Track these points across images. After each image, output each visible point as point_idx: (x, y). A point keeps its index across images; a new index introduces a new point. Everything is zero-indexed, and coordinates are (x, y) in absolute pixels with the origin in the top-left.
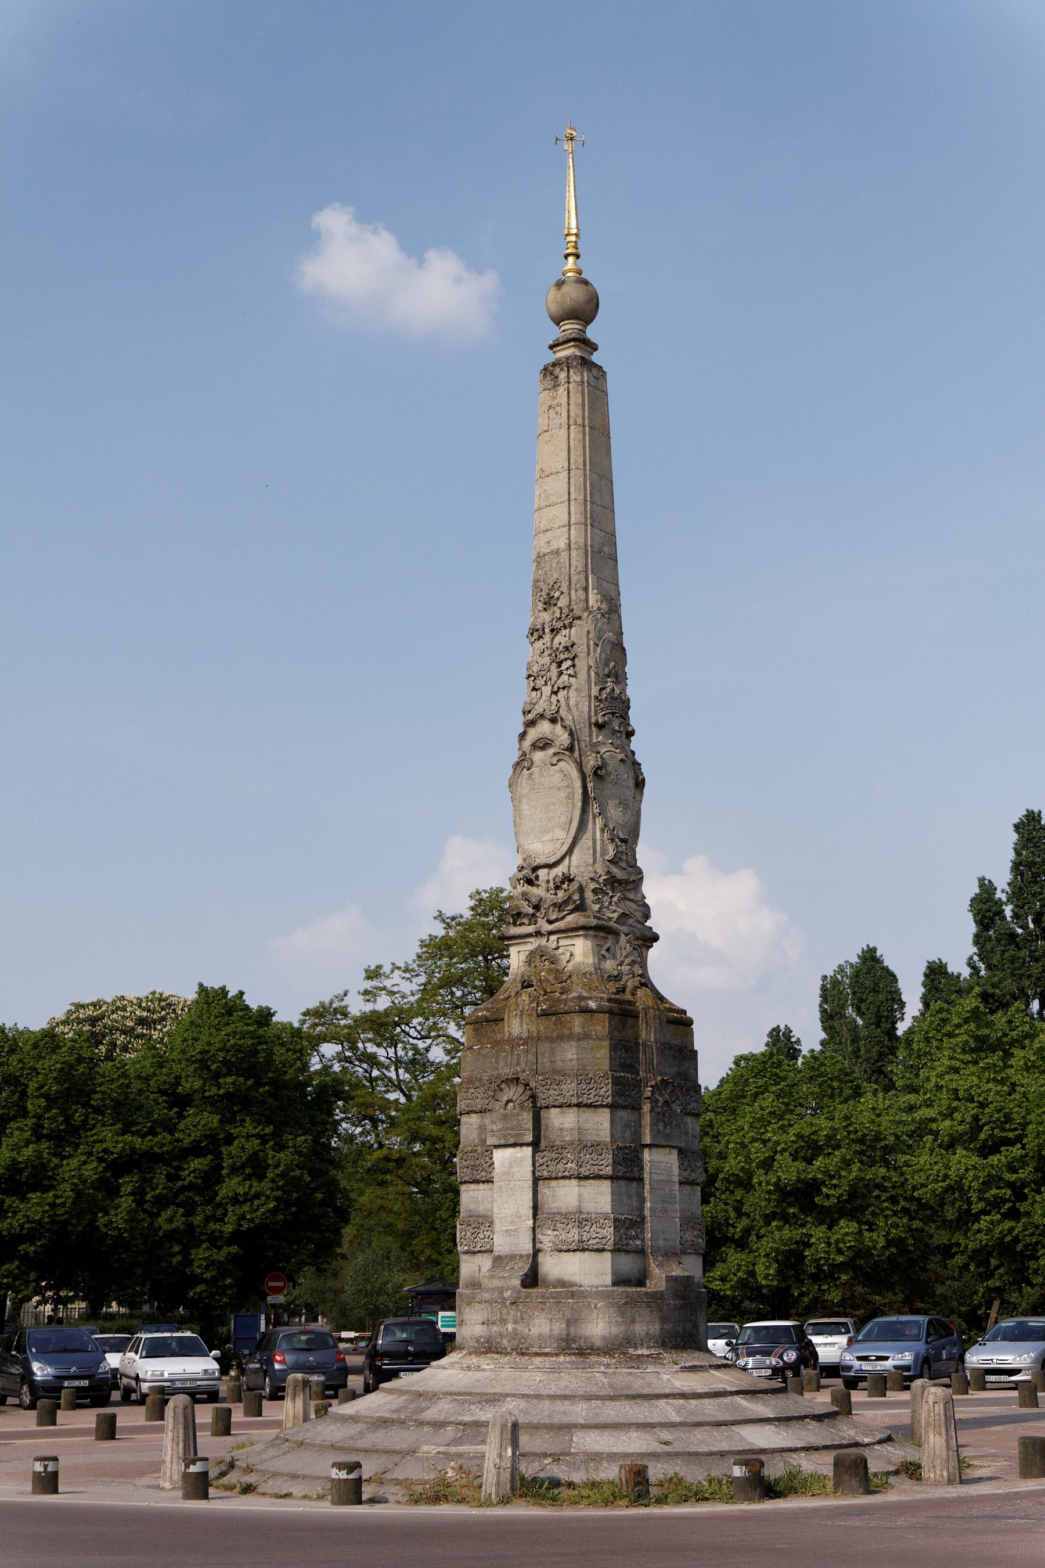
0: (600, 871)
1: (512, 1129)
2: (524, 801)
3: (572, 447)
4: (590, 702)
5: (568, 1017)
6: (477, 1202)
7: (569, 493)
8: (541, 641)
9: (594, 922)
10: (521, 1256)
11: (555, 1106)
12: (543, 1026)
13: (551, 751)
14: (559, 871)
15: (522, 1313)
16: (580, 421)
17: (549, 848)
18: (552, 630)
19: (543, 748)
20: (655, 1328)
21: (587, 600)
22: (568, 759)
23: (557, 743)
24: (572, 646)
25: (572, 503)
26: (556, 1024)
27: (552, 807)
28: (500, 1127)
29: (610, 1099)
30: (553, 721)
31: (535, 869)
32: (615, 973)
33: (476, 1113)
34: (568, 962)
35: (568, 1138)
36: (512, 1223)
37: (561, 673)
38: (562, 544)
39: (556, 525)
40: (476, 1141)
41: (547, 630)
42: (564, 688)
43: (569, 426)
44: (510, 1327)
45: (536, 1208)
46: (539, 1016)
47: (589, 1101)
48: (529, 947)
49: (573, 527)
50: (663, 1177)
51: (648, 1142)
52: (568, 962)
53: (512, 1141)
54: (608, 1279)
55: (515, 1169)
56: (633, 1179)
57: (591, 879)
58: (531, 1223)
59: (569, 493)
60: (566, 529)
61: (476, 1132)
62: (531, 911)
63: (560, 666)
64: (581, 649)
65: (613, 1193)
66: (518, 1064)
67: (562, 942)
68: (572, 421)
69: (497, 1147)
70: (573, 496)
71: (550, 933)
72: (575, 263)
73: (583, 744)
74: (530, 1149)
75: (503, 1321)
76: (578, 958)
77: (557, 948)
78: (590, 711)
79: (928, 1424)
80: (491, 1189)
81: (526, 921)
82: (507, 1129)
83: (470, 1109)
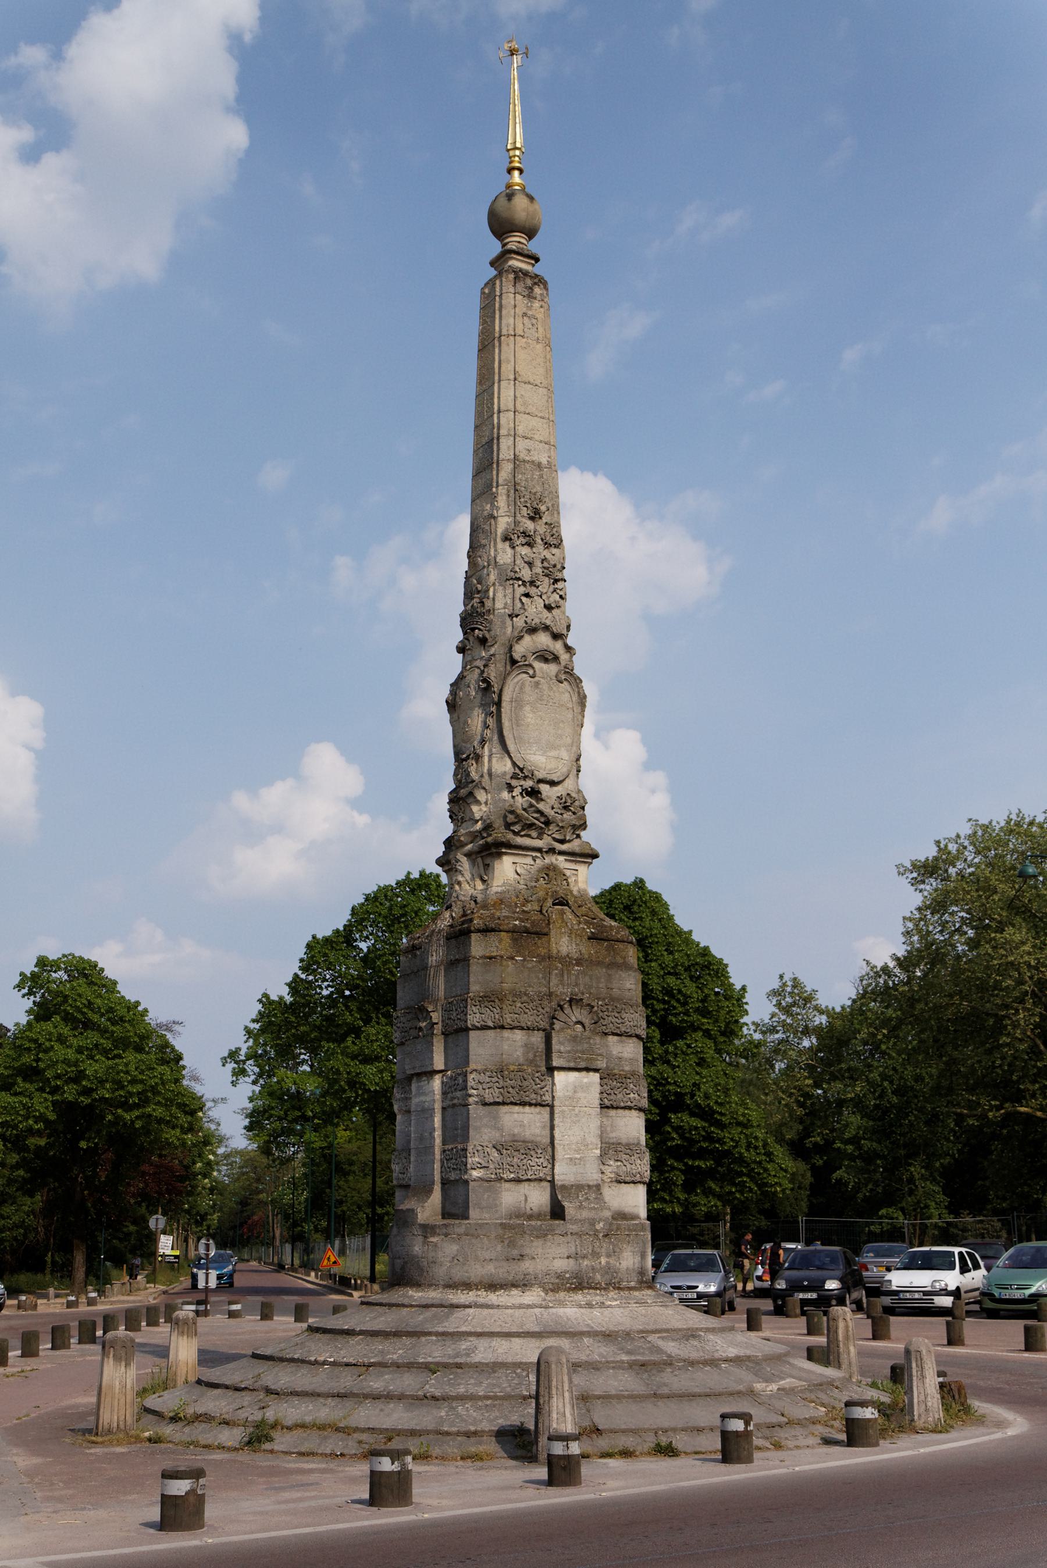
1: (583, 1052)
2: (527, 708)
5: (621, 946)
6: (522, 1126)
10: (589, 1186)
11: (614, 1034)
12: (587, 949)
15: (614, 1245)
17: (552, 765)
19: (546, 661)
26: (607, 949)
27: (561, 725)
28: (568, 1049)
33: (522, 1029)
35: (627, 1068)
36: (577, 1151)
40: (521, 1060)
44: (603, 1260)
46: (589, 938)
53: (583, 1065)
55: (579, 1095)
61: (521, 1050)
66: (577, 985)
75: (596, 1255)
79: (847, 1337)
81: (534, 834)
82: (577, 1051)
83: (517, 1024)
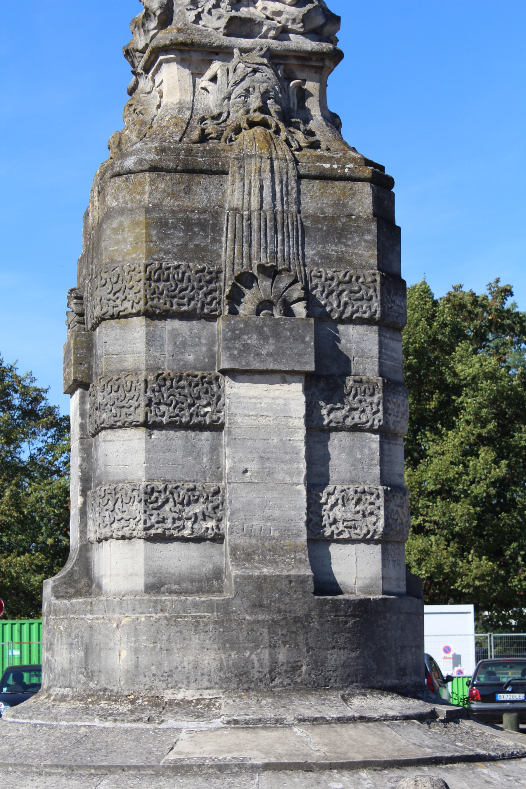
20: (210, 659)
32: (216, 112)
34: (159, 106)
50: (263, 421)
51: (225, 365)
52: (159, 106)
54: (140, 584)
56: (201, 427)
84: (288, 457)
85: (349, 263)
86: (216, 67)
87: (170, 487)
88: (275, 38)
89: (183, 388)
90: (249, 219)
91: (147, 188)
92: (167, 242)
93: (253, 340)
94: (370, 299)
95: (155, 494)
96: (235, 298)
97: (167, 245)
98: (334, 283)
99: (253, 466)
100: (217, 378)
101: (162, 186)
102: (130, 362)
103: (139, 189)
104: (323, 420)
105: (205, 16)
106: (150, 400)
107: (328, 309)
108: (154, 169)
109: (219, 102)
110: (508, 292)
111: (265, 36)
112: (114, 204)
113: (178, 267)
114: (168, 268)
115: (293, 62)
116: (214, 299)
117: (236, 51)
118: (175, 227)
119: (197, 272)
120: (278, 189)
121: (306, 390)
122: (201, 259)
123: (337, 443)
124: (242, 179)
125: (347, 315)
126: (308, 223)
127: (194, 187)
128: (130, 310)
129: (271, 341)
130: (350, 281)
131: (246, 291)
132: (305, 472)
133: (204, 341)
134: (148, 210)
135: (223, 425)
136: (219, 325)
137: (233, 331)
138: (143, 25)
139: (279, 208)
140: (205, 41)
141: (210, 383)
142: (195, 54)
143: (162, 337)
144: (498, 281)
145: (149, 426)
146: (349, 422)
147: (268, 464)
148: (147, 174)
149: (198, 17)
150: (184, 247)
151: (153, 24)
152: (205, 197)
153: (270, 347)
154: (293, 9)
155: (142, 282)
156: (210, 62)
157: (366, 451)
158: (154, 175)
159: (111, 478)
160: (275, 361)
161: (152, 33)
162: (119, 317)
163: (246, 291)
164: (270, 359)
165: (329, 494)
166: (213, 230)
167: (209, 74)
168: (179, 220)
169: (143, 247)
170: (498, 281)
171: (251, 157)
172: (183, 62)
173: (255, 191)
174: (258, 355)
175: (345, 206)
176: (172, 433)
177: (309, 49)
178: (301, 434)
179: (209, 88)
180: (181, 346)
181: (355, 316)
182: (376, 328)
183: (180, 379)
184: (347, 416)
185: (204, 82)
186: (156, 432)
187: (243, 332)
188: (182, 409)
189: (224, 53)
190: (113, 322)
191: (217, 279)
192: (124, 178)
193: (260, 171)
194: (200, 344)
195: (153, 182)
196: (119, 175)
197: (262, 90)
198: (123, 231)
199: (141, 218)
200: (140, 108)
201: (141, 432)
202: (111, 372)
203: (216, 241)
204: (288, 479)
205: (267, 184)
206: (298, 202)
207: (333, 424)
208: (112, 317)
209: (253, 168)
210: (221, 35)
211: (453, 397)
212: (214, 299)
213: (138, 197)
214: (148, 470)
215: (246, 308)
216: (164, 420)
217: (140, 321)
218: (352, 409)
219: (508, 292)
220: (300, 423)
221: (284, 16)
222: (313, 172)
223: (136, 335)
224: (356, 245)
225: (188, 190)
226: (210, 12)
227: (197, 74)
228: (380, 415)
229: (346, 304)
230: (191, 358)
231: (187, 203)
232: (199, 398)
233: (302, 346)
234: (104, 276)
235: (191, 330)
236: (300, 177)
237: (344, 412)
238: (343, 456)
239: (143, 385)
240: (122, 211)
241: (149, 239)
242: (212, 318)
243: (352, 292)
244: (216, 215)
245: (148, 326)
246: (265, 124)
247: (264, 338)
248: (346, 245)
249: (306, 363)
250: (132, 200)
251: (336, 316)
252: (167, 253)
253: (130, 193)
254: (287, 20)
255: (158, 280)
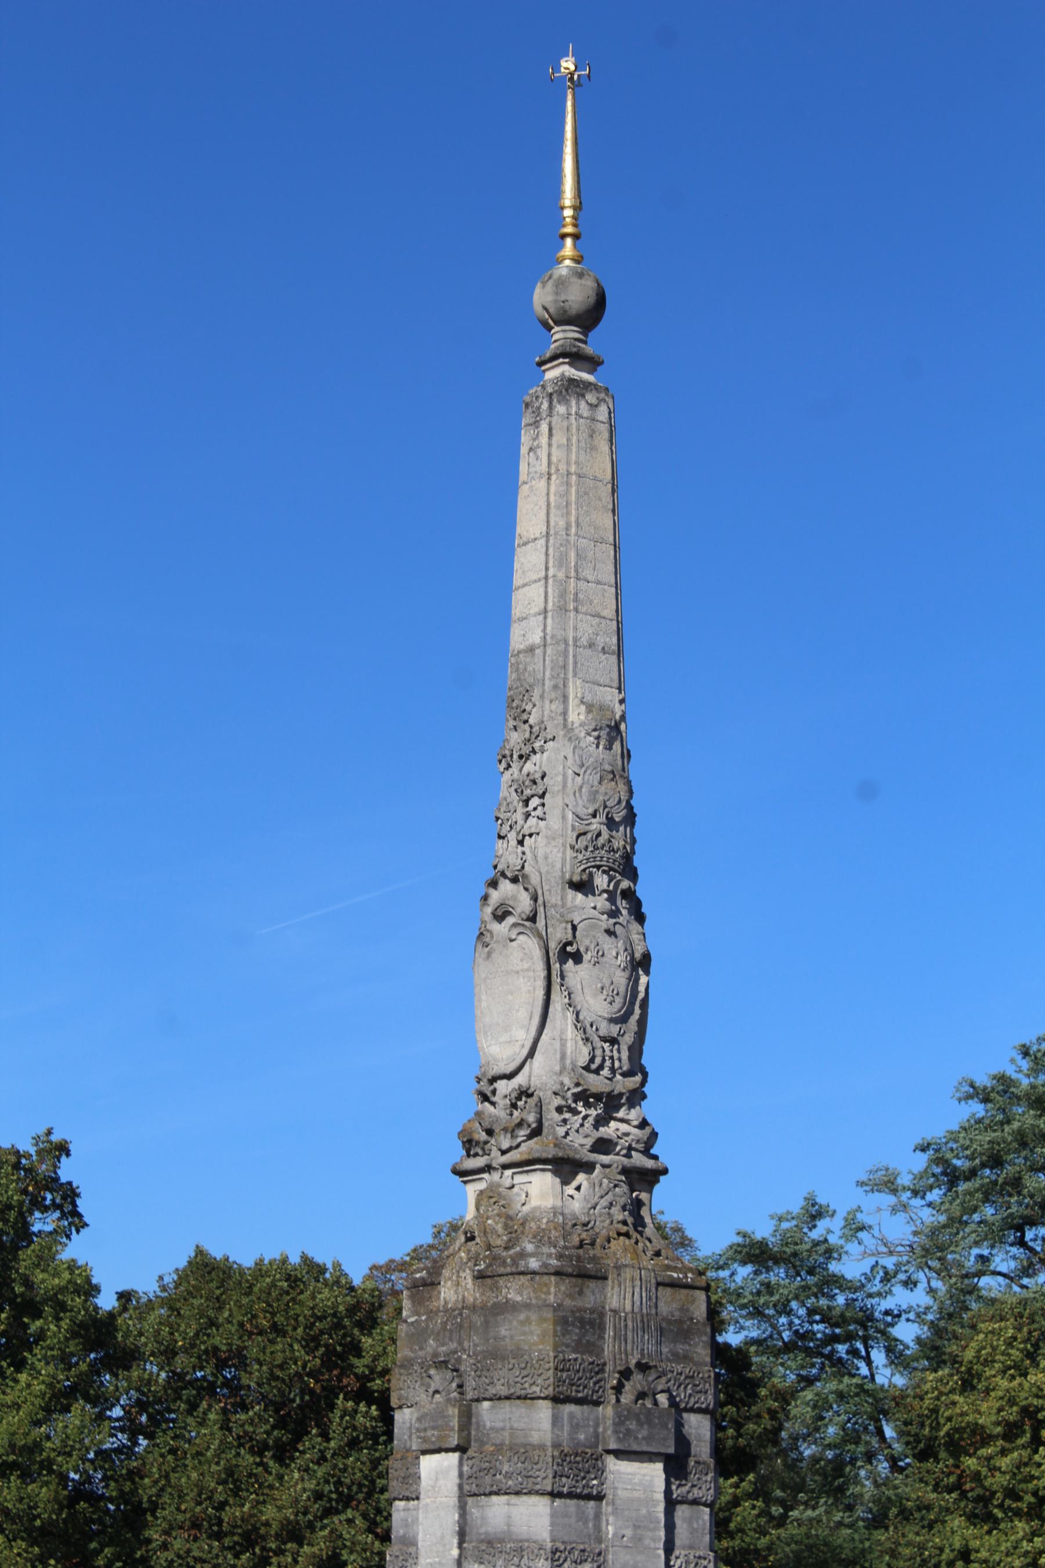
0: (567, 1081)
3: (553, 504)
4: (564, 853)
6: (407, 1526)
7: (547, 569)
8: (511, 771)
9: (551, 1152)
13: (510, 920)
14: (520, 1080)
16: (563, 467)
18: (521, 757)
21: (565, 713)
22: (528, 932)
23: (519, 910)
24: (543, 778)
25: (550, 581)
29: (551, 1389)
30: (515, 880)
31: (493, 1080)
32: (584, 1219)
37: (527, 815)
38: (536, 638)
39: (532, 612)
41: (515, 757)
42: (531, 835)
43: (549, 474)
45: (462, 1535)
47: (523, 1392)
48: (482, 1186)
49: (550, 614)
50: (636, 1494)
51: (613, 1446)
52: (524, 1204)
55: (441, 1482)
56: (589, 1497)
57: (555, 1094)
58: (455, 1552)
59: (547, 569)
60: (541, 618)
62: (483, 1136)
63: (527, 806)
64: (553, 782)
65: (553, 1515)
67: (519, 1179)
68: (553, 471)
69: (425, 1452)
70: (551, 573)
71: (505, 1167)
72: (575, 245)
73: (552, 912)
74: (457, 1455)
76: (534, 1202)
77: (513, 1186)
78: (563, 865)
80: (417, 1509)
84: (652, 1526)
85: (691, 1360)
86: (581, 1178)
87: (568, 1548)
88: (624, 1156)
89: (578, 1463)
90: (625, 1320)
91: (552, 1290)
92: (568, 1337)
93: (632, 1425)
94: (706, 1392)
95: (558, 1554)
96: (618, 1389)
97: (567, 1340)
98: (682, 1378)
99: (628, 1533)
100: (601, 1456)
101: (563, 1288)
102: (535, 1438)
103: (544, 1289)
104: (672, 1494)
105: (572, 1133)
106: (556, 1472)
107: (678, 1399)
108: (558, 1273)
109: (586, 1211)
110: (63, 1149)
111: (618, 1154)
112: (519, 1298)
113: (576, 1360)
114: (569, 1360)
115: (635, 1176)
116: (600, 1387)
117: (598, 1166)
118: (573, 1325)
119: (590, 1364)
120: (644, 1295)
121: (666, 1470)
122: (591, 1353)
123: (682, 1512)
124: (620, 1286)
125: (690, 1405)
126: (664, 1325)
127: (585, 1290)
128: (538, 1394)
129: (646, 1427)
130: (693, 1377)
131: (626, 1383)
132: (663, 1538)
133: (591, 1423)
134: (555, 1310)
135: (604, 1497)
136: (607, 1411)
137: (619, 1417)
138: (513, 1131)
139: (644, 1311)
140: (577, 1157)
141: (596, 1460)
142: (566, 1167)
143: (563, 1419)
144: (49, 1132)
145: (554, 1495)
146: (690, 1497)
147: (639, 1532)
148: (553, 1278)
149: (567, 1134)
150: (579, 1342)
151: (523, 1132)
152: (592, 1298)
153: (644, 1432)
154: (636, 1131)
155: (551, 1371)
156: (576, 1174)
157: (701, 1522)
158: (558, 1278)
159: (514, 1537)
160: (648, 1444)
161: (520, 1139)
162: (526, 1398)
163: (626, 1383)
164: (644, 1442)
165: (677, 1558)
166: (599, 1328)
167: (575, 1184)
168: (576, 1318)
169: (550, 1340)
170: (49, 1132)
171: (626, 1266)
172: (556, 1173)
173: (629, 1296)
174: (636, 1438)
175: (688, 1310)
176: (568, 1501)
177: (649, 1167)
178: (661, 1507)
179: (576, 1197)
180: (575, 1427)
181: (696, 1406)
182: (708, 1416)
183: (576, 1455)
184: (689, 1492)
185: (570, 1190)
186: (557, 1500)
187: (627, 1418)
188: (577, 1481)
189: (588, 1167)
190: (518, 1402)
191: (602, 1371)
192: (529, 1277)
193: (633, 1280)
194: (588, 1426)
195: (557, 1284)
196: (523, 1273)
197: (622, 1204)
198: (530, 1324)
199: (550, 1315)
200: (502, 1202)
201: (545, 1500)
202: (516, 1445)
203: (601, 1337)
204: (652, 1545)
205: (637, 1290)
206: (656, 1307)
207: (679, 1498)
208: (519, 1398)
209: (628, 1276)
210: (585, 1151)
211: (26, 1320)
212: (600, 1387)
213: (543, 1296)
214: (551, 1531)
215: (627, 1398)
216: (565, 1490)
217: (547, 1404)
218: (693, 1486)
219: (63, 1149)
220: (661, 1497)
221: (631, 1137)
222: (666, 1281)
223: (542, 1415)
224: (696, 1345)
225: (581, 1293)
226: (577, 1131)
227: (565, 1182)
228: (712, 1491)
229: (690, 1395)
230: (582, 1437)
231: (579, 1303)
232: (588, 1472)
233: (666, 1432)
234: (513, 1361)
235: (582, 1413)
236: (658, 1284)
237: (687, 1488)
238: (685, 1526)
239: (550, 1460)
240: (527, 1306)
241: (555, 1335)
242: (597, 1403)
243: (695, 1385)
244: (602, 1315)
245: (553, 1408)
246: (627, 1235)
247: (640, 1424)
248: (690, 1345)
249: (668, 1447)
250: (537, 1298)
251: (683, 1405)
252: (567, 1346)
253: (535, 1291)
254: (633, 1140)
255: (562, 1370)
